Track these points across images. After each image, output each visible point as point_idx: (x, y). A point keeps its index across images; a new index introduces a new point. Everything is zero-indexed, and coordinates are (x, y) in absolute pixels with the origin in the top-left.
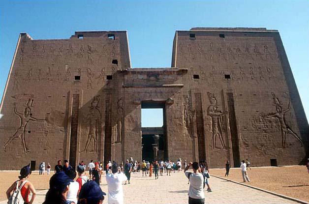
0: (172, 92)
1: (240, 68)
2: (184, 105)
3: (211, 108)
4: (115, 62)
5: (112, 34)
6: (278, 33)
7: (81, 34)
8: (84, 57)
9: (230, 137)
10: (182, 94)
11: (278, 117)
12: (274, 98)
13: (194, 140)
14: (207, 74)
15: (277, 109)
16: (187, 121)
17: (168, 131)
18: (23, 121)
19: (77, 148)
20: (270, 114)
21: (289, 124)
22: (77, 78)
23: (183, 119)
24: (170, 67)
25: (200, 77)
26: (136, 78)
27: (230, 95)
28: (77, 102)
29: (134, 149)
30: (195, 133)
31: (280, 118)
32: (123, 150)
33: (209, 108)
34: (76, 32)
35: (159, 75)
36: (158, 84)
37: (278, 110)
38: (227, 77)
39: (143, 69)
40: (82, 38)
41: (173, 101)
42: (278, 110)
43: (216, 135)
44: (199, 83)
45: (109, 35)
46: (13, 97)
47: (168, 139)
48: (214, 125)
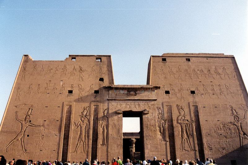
1: (203, 85)
3: (180, 118)
4: (102, 80)
5: (99, 57)
6: (234, 58)
8: (76, 75)
9: (196, 142)
10: (156, 106)
11: (236, 125)
12: (232, 110)
14: (176, 90)
16: (160, 128)
17: (145, 136)
18: (23, 127)
19: (69, 150)
22: (70, 92)
25: (170, 92)
27: (196, 107)
28: (70, 112)
29: (117, 151)
30: (167, 138)
32: (107, 151)
33: (178, 117)
34: (70, 56)
36: (136, 98)
38: (193, 92)
40: (74, 60)
41: (149, 111)
43: (184, 140)
44: (169, 97)
45: (97, 59)
47: (145, 142)
48: (182, 132)
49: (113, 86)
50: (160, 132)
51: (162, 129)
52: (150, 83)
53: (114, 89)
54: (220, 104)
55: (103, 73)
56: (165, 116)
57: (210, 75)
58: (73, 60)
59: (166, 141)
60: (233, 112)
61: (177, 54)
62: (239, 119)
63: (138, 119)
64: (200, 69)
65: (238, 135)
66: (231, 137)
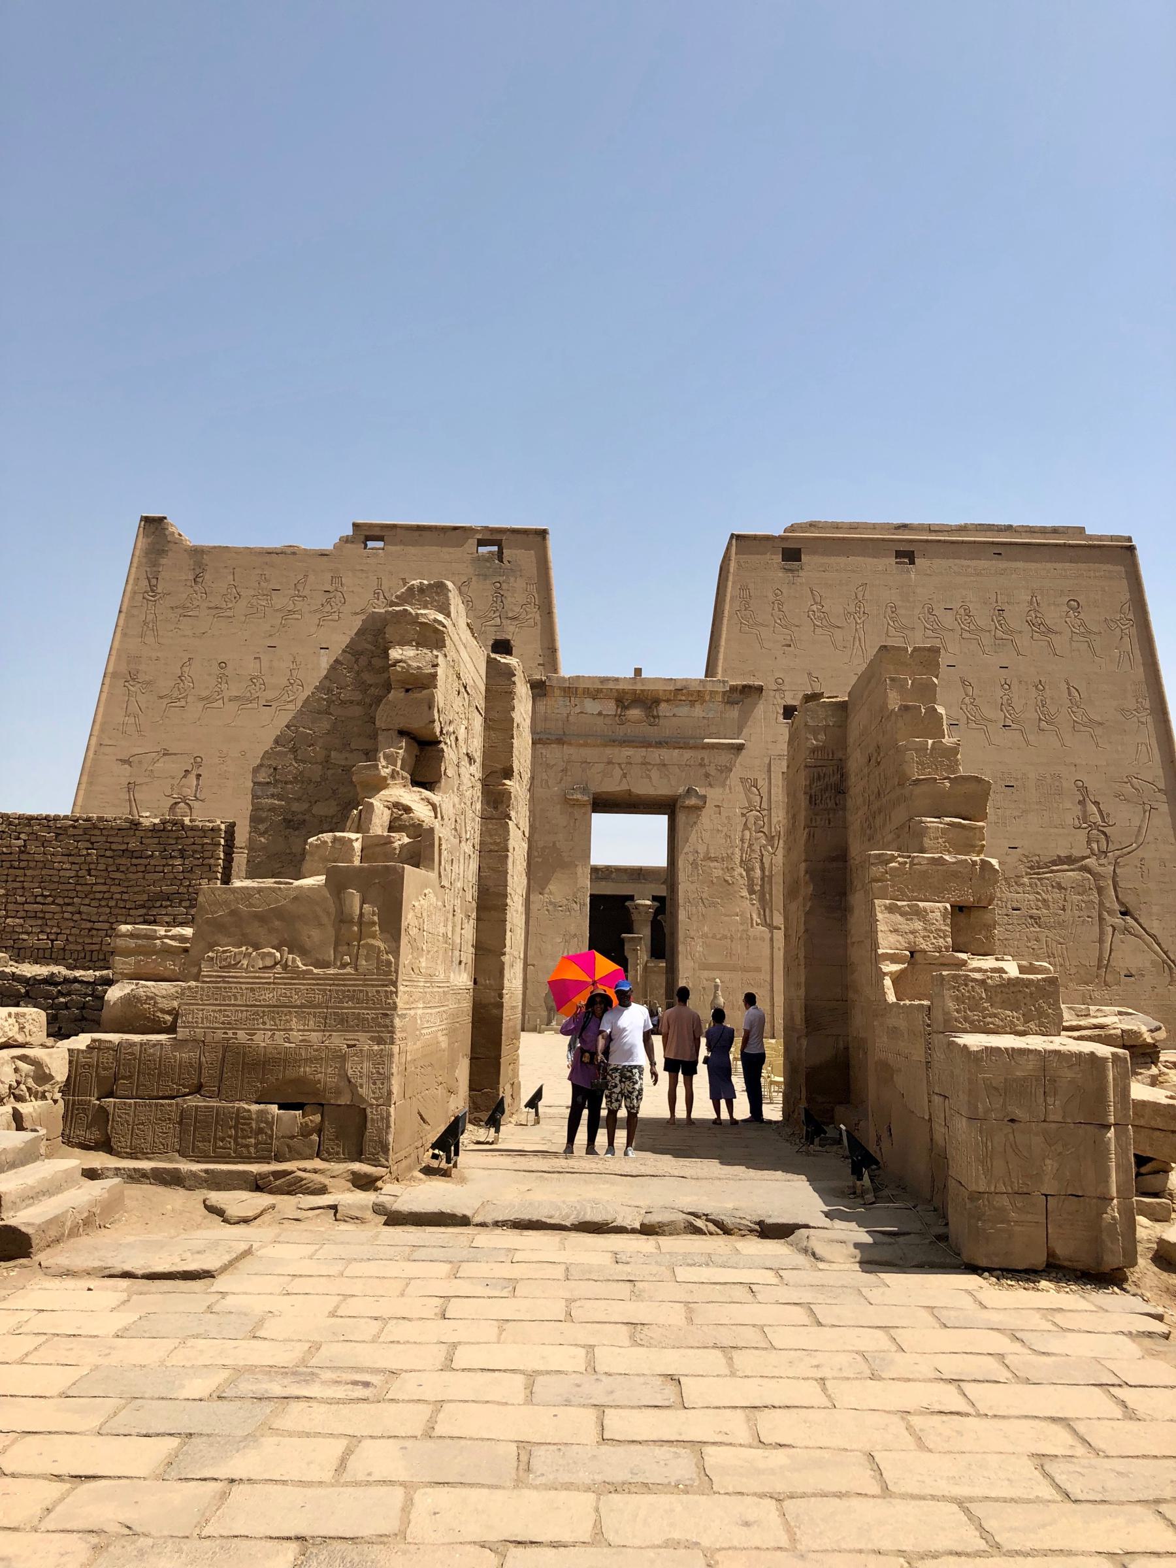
0: (700, 765)
2: (743, 815)
6: (1132, 549)
7: (377, 533)
11: (1089, 871)
13: (772, 939)
16: (748, 871)
20: (1060, 861)
23: (738, 861)
24: (700, 674)
31: (1096, 876)
34: (355, 525)
35: (657, 701)
36: (651, 732)
37: (1095, 846)
40: (380, 544)
41: (705, 797)
42: (1095, 846)
45: (481, 543)
46: (124, 761)
49: (554, 683)
50: (751, 892)
51: (758, 872)
53: (557, 692)
55: (510, 615)
56: (774, 820)
57: (999, 634)
58: (370, 544)
59: (772, 928)
60: (1085, 812)
61: (853, 527)
62: (1111, 847)
63: (661, 822)
64: (955, 605)
65: (1095, 914)
66: (1061, 924)
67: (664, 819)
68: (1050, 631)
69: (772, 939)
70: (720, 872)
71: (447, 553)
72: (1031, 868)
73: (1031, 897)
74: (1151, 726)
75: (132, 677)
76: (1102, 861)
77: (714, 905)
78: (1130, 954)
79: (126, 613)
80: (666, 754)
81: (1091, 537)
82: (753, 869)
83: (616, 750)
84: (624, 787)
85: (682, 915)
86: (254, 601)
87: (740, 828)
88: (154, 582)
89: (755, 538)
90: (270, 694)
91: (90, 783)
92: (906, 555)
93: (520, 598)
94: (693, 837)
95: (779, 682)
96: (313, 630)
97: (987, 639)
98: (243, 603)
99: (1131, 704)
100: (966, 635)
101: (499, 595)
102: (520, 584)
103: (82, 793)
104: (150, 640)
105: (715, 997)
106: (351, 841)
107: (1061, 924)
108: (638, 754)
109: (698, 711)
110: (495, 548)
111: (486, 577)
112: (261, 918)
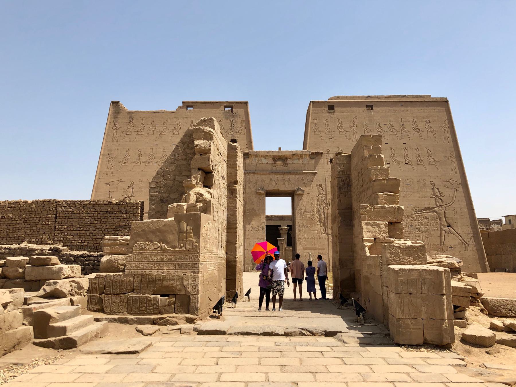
1: (391, 149)
2: (317, 196)
6: (447, 102)
7: (191, 105)
11: (436, 212)
12: (433, 189)
13: (328, 238)
15: (436, 202)
16: (320, 215)
20: (426, 209)
21: (450, 222)
24: (301, 149)
26: (260, 162)
34: (183, 102)
35: (286, 159)
37: (438, 203)
39: (269, 152)
40: (192, 108)
42: (438, 203)
45: (226, 107)
46: (107, 184)
49: (252, 153)
50: (321, 222)
51: (323, 216)
52: (308, 147)
53: (253, 156)
54: (416, 180)
56: (328, 198)
57: (403, 132)
58: (189, 109)
59: (328, 234)
61: (352, 97)
66: (427, 231)
67: (290, 198)
68: (420, 130)
69: (328, 238)
70: (310, 216)
71: (214, 110)
72: (416, 212)
73: (417, 222)
74: (456, 162)
75: (109, 155)
76: (441, 209)
77: (308, 227)
78: (451, 240)
79: (107, 134)
80: (290, 176)
81: (433, 98)
82: (321, 215)
83: (273, 175)
84: (276, 188)
85: (297, 231)
86: (150, 129)
87: (316, 201)
88: (116, 123)
89: (318, 102)
90: (156, 160)
91: (96, 192)
92: (370, 106)
93: (239, 125)
94: (300, 204)
95: (328, 151)
96: (170, 138)
97: (398, 134)
98: (146, 129)
99: (448, 155)
100: (391, 133)
101: (232, 124)
102: (239, 120)
103: (93, 195)
104: (115, 143)
105: (309, 259)
106: (183, 205)
107: (427, 231)
108: (280, 177)
109: (301, 161)
110: (231, 109)
111: (227, 118)
112: (153, 232)
